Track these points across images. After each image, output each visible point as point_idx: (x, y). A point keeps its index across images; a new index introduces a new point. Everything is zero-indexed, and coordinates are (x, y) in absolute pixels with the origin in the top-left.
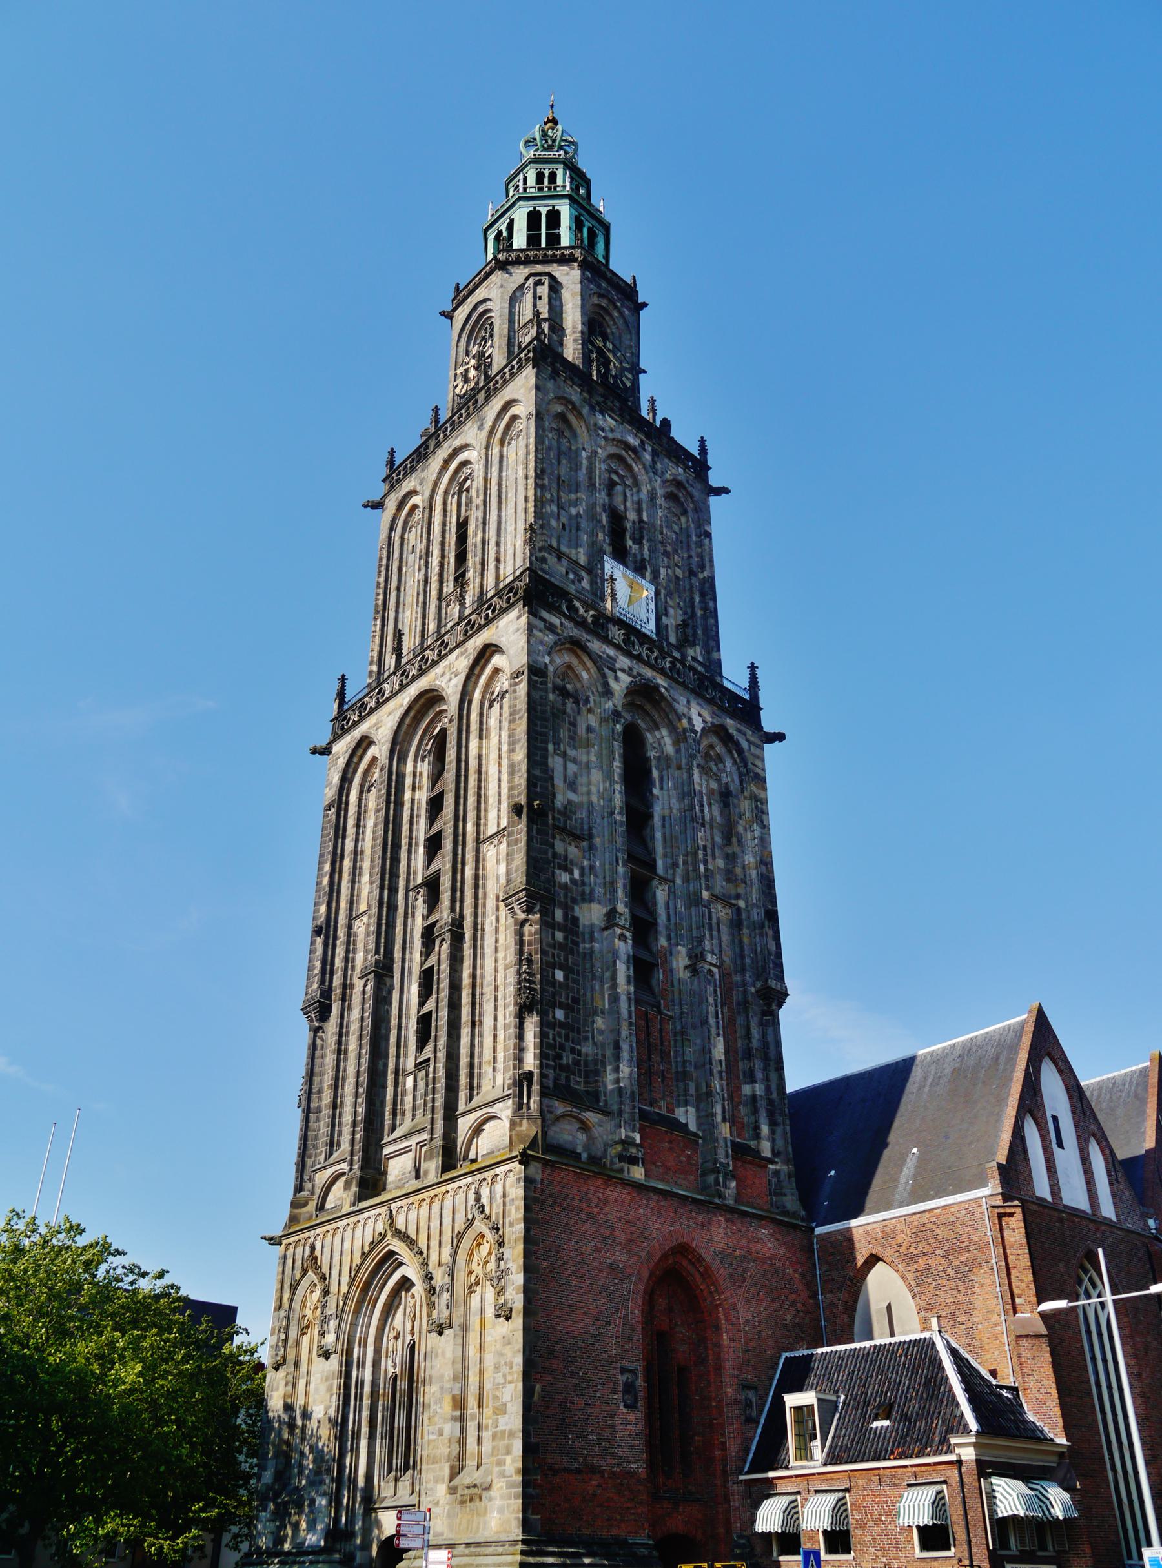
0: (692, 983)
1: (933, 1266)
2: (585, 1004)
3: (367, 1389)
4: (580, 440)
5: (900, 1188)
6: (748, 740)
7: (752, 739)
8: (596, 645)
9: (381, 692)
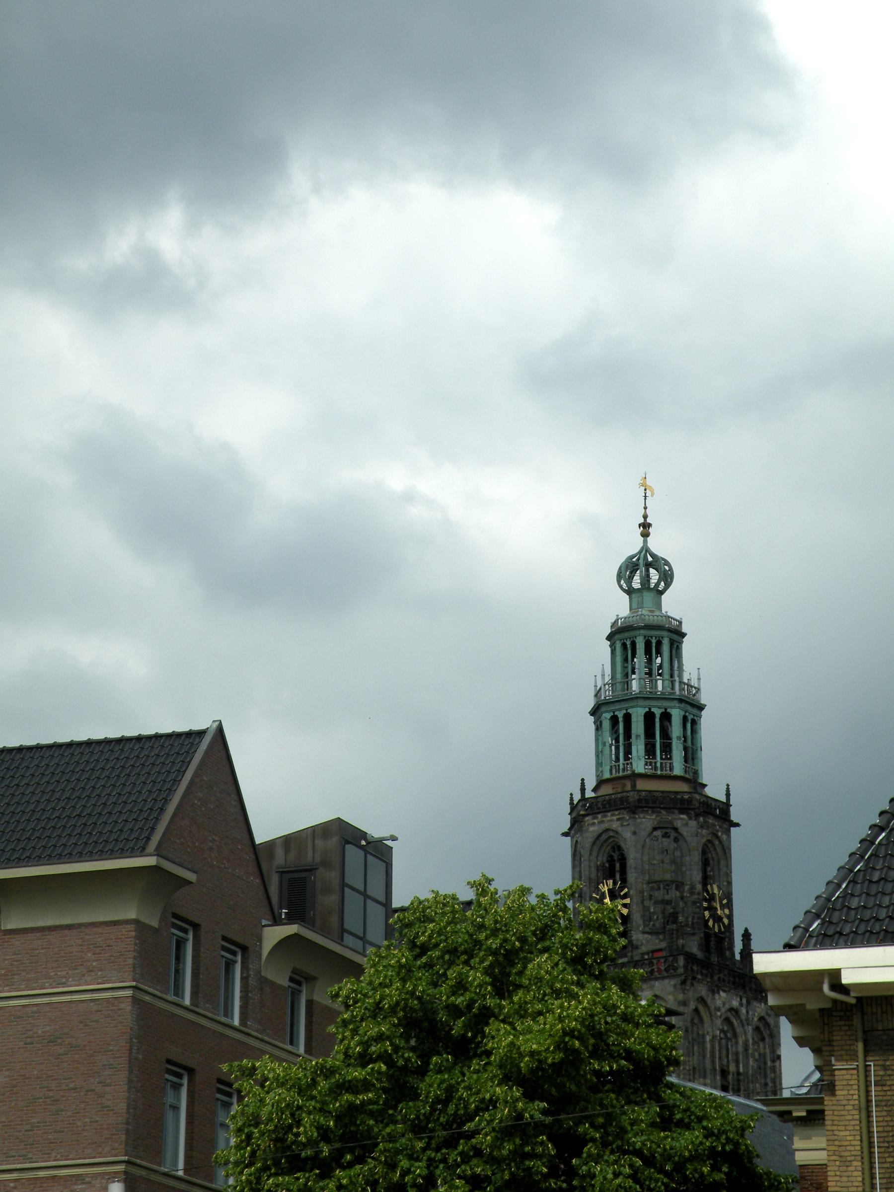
4: (706, 1025)
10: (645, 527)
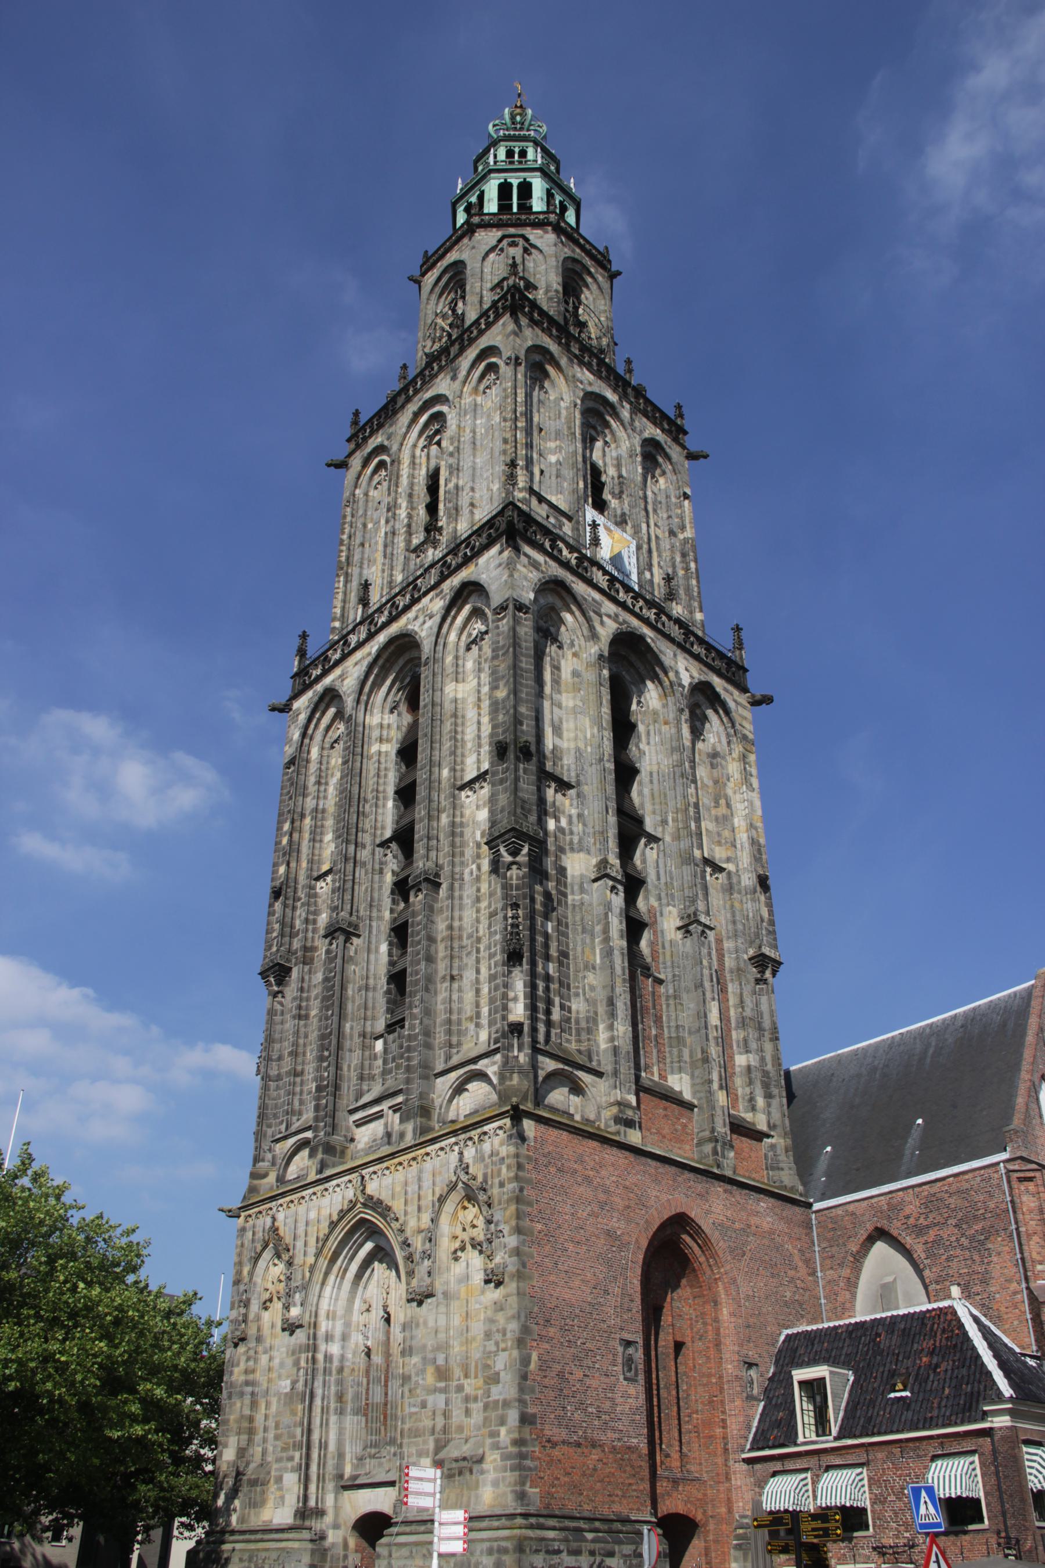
0: (684, 945)
1: (945, 1236)
2: (575, 959)
3: (336, 1363)
5: (906, 1159)
6: (735, 701)
7: (739, 700)
8: (580, 588)
9: (346, 643)
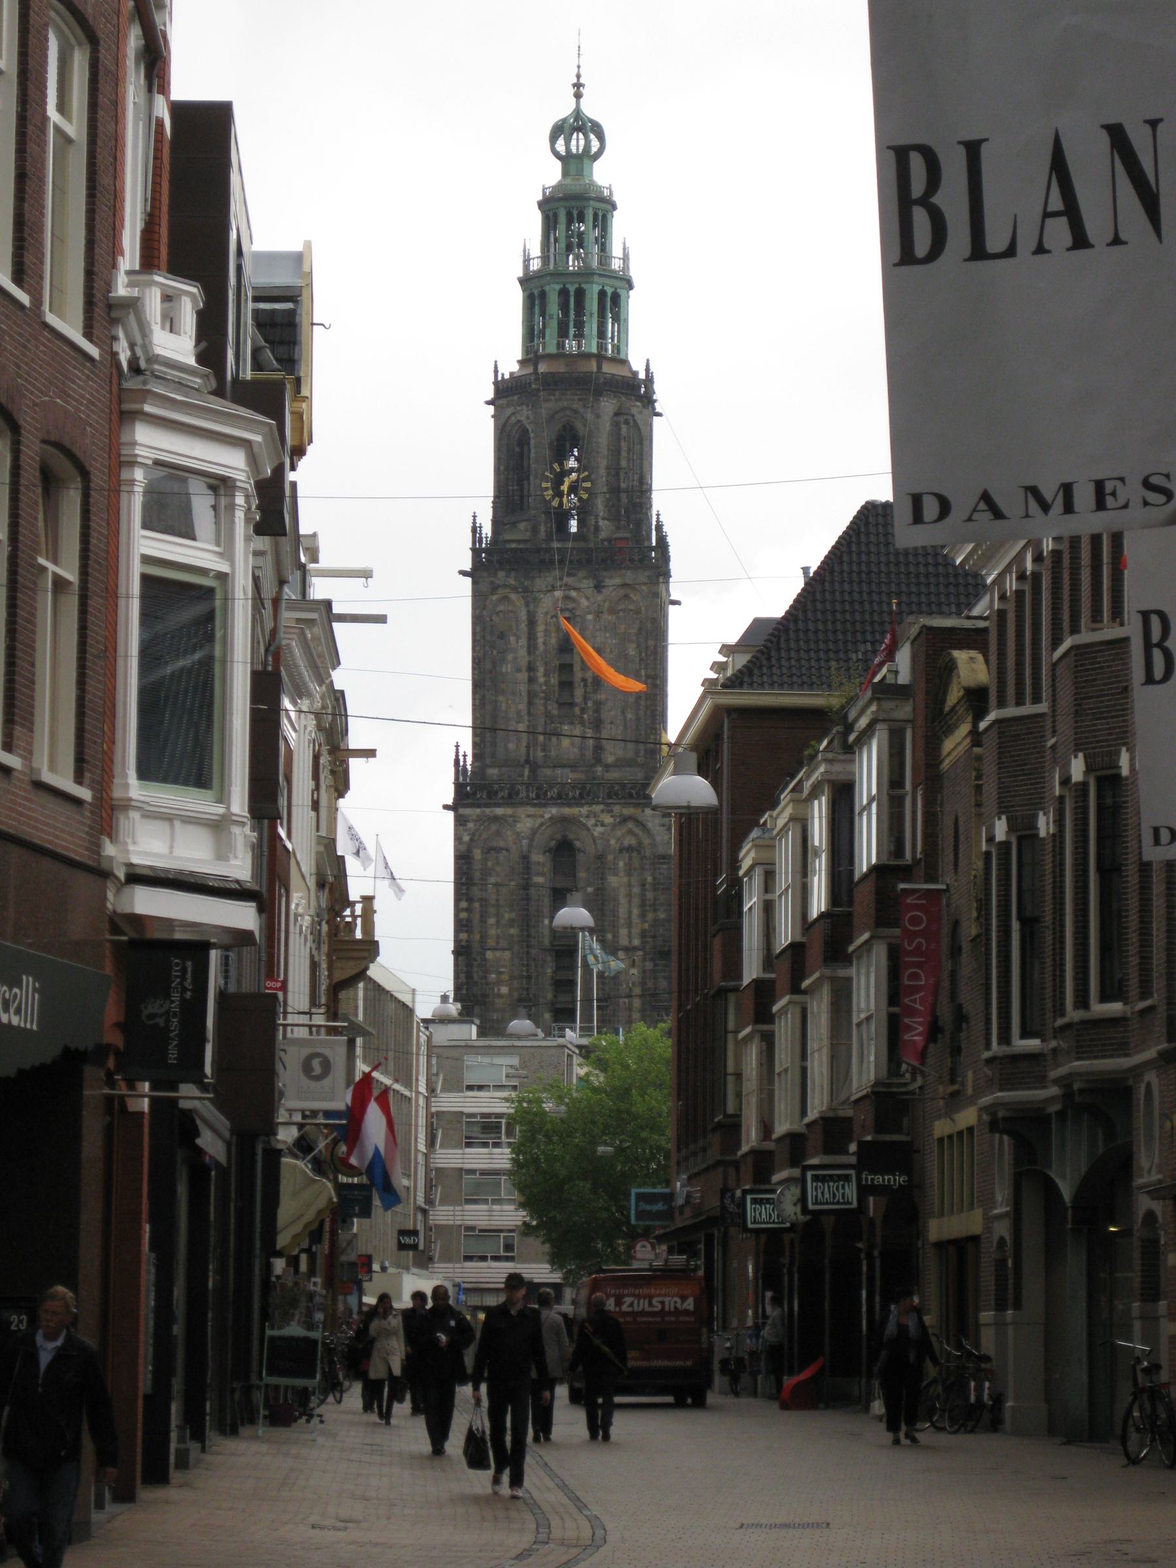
10: (578, 86)
